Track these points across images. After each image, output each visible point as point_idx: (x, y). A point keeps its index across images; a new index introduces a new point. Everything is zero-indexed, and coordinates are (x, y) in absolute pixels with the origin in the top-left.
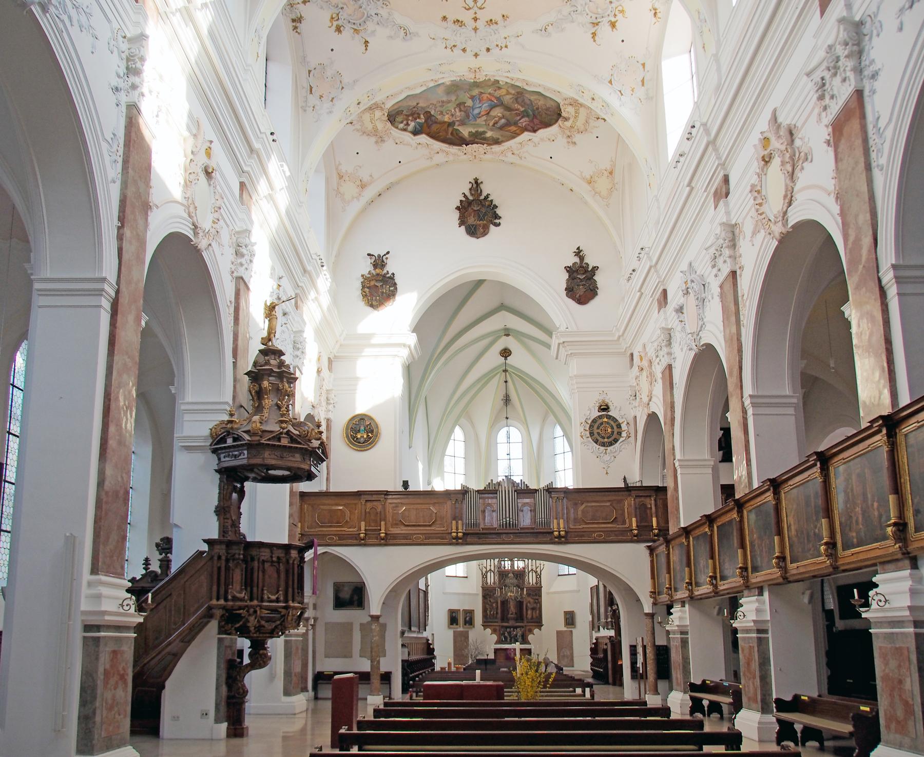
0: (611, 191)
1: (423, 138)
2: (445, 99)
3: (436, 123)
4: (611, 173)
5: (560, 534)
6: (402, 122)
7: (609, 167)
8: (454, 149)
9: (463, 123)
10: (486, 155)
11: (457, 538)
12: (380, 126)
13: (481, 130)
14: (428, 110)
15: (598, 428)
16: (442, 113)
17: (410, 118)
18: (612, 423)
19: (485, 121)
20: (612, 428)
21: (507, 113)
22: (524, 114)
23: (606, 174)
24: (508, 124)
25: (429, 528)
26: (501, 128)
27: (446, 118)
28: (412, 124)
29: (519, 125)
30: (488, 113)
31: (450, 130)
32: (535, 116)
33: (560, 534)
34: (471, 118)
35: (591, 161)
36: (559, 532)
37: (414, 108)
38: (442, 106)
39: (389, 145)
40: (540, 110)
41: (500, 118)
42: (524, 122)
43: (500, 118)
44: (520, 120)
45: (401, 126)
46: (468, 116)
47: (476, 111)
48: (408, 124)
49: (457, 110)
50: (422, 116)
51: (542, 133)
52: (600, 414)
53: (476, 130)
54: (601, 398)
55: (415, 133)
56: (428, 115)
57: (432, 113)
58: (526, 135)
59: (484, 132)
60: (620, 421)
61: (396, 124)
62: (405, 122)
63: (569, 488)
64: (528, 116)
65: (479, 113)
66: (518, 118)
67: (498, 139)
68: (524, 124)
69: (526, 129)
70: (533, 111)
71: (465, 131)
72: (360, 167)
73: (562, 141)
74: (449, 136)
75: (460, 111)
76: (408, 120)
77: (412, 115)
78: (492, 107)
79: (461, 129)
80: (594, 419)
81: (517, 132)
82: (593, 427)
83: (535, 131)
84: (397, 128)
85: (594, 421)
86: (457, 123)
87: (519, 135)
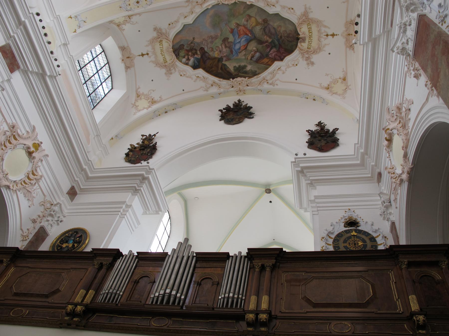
0: (345, 90)
1: (200, 72)
2: (213, 34)
3: (209, 58)
4: (344, 79)
5: (257, 318)
6: (184, 57)
7: (342, 76)
8: (224, 83)
9: (228, 59)
10: (248, 87)
11: (73, 314)
12: (168, 58)
13: (242, 64)
14: (202, 46)
15: (345, 241)
16: (212, 50)
17: (190, 53)
18: (364, 237)
19: (245, 55)
20: (364, 241)
21: (260, 47)
22: (272, 45)
23: (340, 81)
24: (261, 57)
25: (44, 300)
26: (257, 61)
27: (216, 54)
28: (192, 59)
29: (270, 56)
30: (246, 48)
31: (220, 65)
32: (280, 45)
33: (257, 318)
34: (234, 54)
35: (327, 75)
36: (257, 314)
37: (192, 43)
38: (212, 42)
39: (175, 75)
40: (283, 38)
41: (256, 52)
42: (273, 53)
43: (256, 52)
44: (270, 51)
45: (184, 60)
46: (232, 52)
47: (237, 47)
48: (188, 59)
49: (223, 47)
50: (198, 53)
51: (288, 59)
52: (347, 229)
53: (239, 64)
54: (347, 215)
55: (195, 67)
56: (203, 52)
57: (206, 49)
58: (277, 64)
59: (245, 67)
60: (374, 235)
61: (180, 58)
62: (186, 57)
63: (284, 250)
64: (275, 46)
65: (240, 49)
66: (269, 49)
67: (256, 71)
68: (273, 55)
69: (274, 60)
70: (278, 40)
71: (231, 66)
72: (153, 91)
73: (303, 63)
74: (220, 71)
75: (226, 47)
76: (188, 55)
77: (191, 50)
78: (249, 41)
79: (227, 63)
80: (339, 234)
81: (269, 63)
82: (338, 241)
83: (282, 59)
84: (181, 61)
85: (340, 235)
86: (224, 59)
87: (270, 65)
